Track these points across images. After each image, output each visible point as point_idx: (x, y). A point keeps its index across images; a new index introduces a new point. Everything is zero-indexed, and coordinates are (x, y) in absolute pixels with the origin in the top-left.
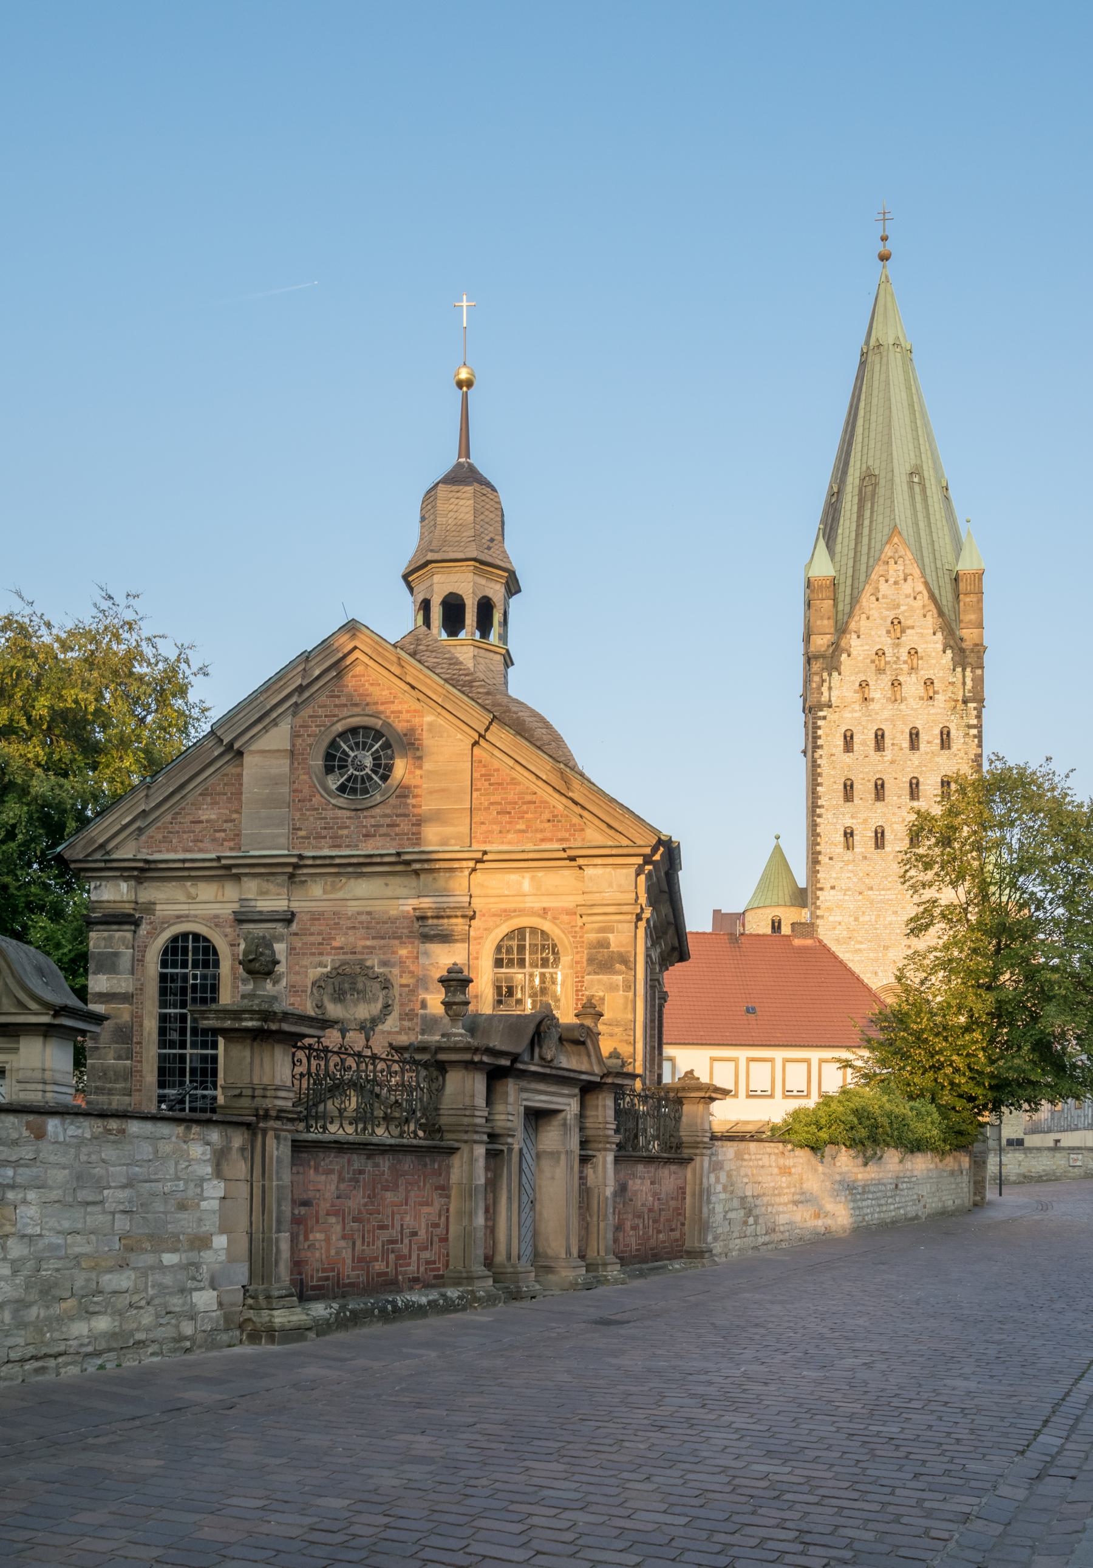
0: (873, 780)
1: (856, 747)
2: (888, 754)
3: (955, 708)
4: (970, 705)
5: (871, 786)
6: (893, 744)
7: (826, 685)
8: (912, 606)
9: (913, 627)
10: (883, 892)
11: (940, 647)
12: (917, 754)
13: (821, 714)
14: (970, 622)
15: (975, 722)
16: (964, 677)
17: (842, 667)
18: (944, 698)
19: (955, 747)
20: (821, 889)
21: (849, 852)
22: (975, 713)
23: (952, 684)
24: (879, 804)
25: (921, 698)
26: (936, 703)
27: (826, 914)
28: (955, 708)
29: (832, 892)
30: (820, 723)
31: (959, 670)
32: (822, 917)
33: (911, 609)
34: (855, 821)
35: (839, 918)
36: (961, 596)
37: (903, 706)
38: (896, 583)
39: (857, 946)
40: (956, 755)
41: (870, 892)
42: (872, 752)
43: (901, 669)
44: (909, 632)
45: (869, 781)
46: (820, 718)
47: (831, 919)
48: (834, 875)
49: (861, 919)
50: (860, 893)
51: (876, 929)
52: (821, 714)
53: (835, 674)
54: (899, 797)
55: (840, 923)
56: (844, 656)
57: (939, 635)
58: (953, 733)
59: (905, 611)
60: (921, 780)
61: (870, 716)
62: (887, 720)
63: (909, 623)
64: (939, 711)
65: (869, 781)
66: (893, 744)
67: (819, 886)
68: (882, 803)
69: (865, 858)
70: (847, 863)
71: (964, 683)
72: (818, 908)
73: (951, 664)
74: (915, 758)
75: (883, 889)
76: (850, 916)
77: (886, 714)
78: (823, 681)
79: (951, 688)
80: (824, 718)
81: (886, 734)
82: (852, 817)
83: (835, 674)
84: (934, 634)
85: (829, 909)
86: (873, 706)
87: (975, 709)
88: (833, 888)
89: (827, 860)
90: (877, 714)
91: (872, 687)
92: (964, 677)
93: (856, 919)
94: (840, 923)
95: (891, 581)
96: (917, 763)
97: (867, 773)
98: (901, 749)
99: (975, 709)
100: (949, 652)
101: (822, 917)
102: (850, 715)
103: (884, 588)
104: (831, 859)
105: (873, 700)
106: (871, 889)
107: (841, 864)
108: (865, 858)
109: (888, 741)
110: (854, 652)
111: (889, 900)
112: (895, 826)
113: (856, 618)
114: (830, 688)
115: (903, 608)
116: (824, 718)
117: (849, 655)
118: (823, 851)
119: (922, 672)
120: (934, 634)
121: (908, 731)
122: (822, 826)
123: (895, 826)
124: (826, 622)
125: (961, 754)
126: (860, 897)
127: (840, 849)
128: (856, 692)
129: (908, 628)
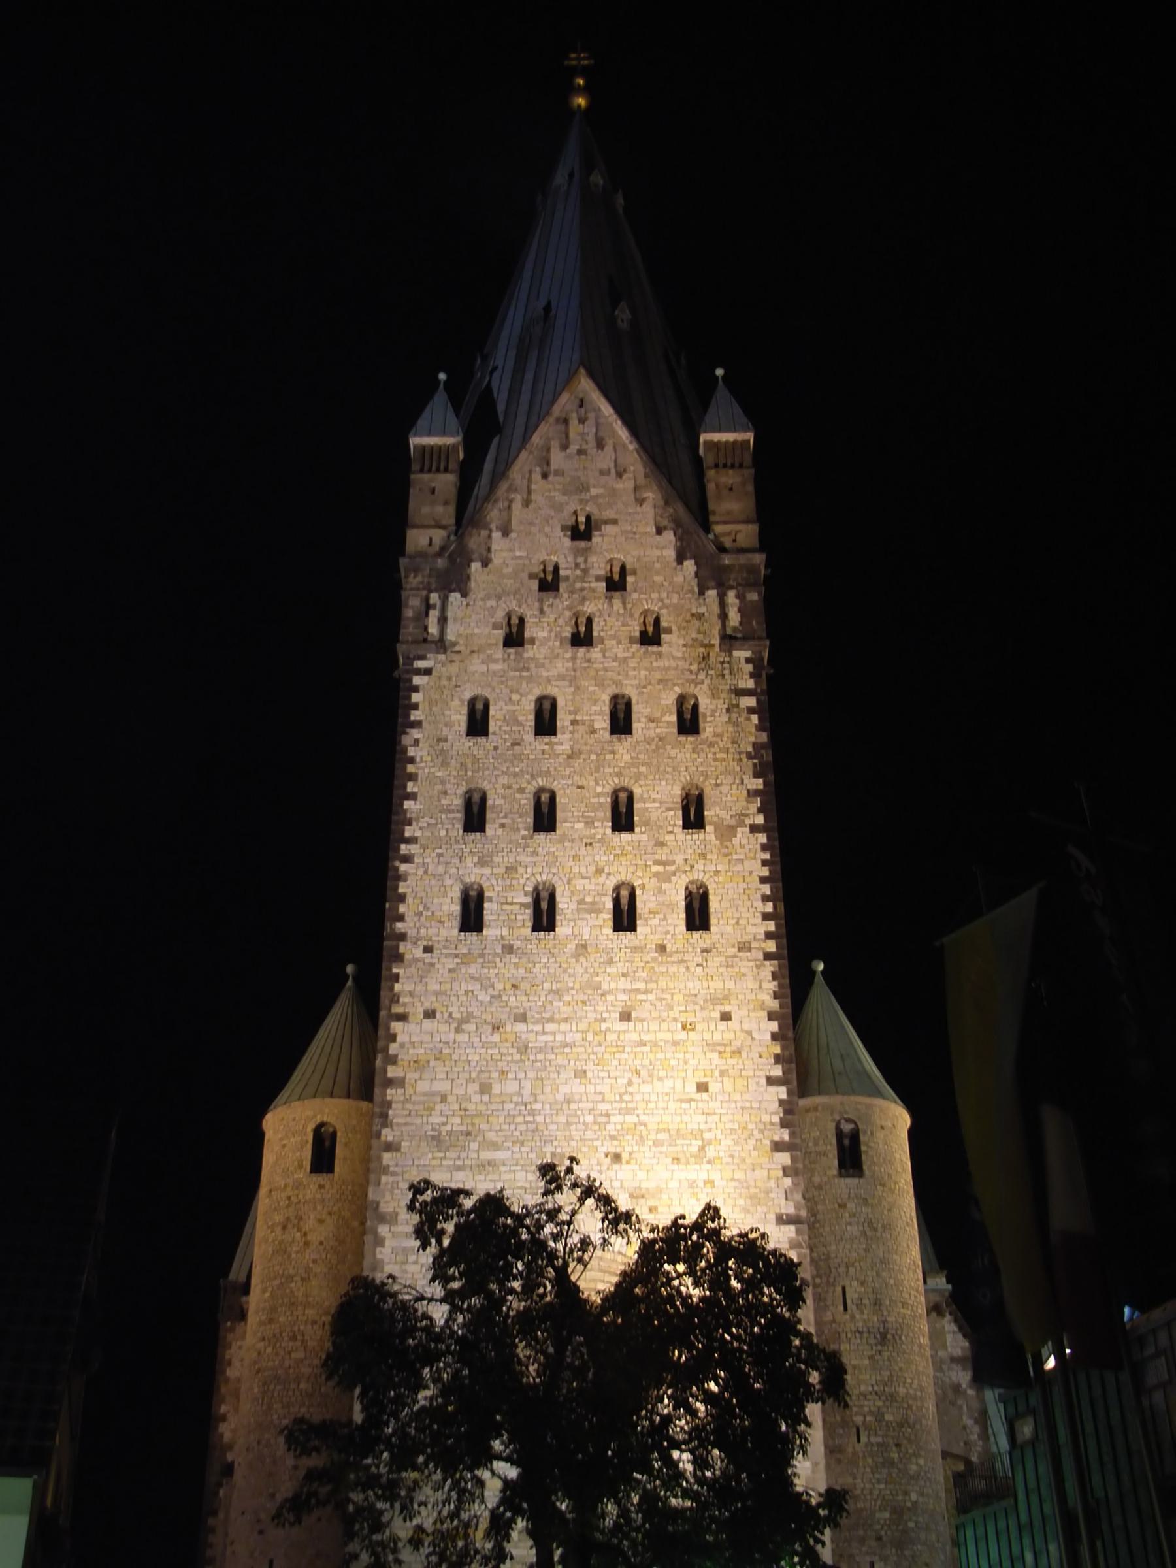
0: (531, 789)
1: (493, 726)
2: (563, 741)
3: (705, 658)
4: (736, 653)
5: (526, 802)
6: (574, 723)
7: (434, 615)
8: (614, 490)
9: (614, 522)
10: (550, 1027)
11: (671, 554)
12: (628, 741)
13: (420, 664)
14: (729, 513)
15: (750, 684)
16: (723, 605)
17: (473, 584)
18: (682, 642)
19: (708, 730)
20: (402, 1018)
21: (472, 937)
22: (750, 667)
23: (699, 617)
24: (541, 837)
25: (632, 640)
26: (664, 648)
27: (411, 1076)
28: (705, 658)
29: (428, 1024)
30: (417, 680)
31: (712, 593)
32: (400, 1083)
33: (613, 493)
34: (487, 871)
35: (442, 1086)
36: (711, 474)
37: (595, 653)
38: (580, 452)
39: (486, 1155)
40: (711, 745)
41: (520, 1027)
42: (529, 736)
43: (593, 590)
44: (608, 529)
45: (521, 790)
46: (419, 672)
47: (423, 1086)
48: (436, 987)
49: (496, 1089)
50: (496, 1028)
51: (532, 1113)
52: (420, 664)
53: (455, 597)
54: (589, 823)
55: (444, 1098)
56: (475, 566)
57: (669, 536)
58: (705, 704)
59: (598, 496)
60: (637, 791)
61: (528, 669)
62: (561, 677)
63: (609, 514)
64: (673, 664)
65: (521, 790)
66: (574, 723)
67: (397, 1009)
68: (551, 836)
69: (509, 949)
70: (466, 959)
71: (724, 616)
72: (393, 1060)
73: (694, 582)
74: (624, 748)
75: (551, 1020)
76: (470, 1080)
77: (560, 667)
78: (428, 607)
79: (697, 623)
80: (428, 672)
81: (561, 703)
82: (482, 863)
83: (455, 597)
84: (659, 531)
85: (418, 1065)
86: (529, 652)
87: (748, 661)
88: (430, 1014)
89: (418, 953)
90: (543, 665)
91: (530, 621)
92: (723, 605)
93: (485, 1089)
94: (444, 1098)
95: (574, 448)
96: (627, 757)
97: (515, 775)
98: (594, 731)
99: (748, 661)
100: (690, 566)
101: (400, 1083)
102: (484, 668)
103: (557, 459)
104: (428, 950)
105: (532, 641)
106: (522, 1018)
107: (450, 963)
108: (509, 949)
109: (563, 719)
110: (496, 560)
111: (566, 1045)
112: (580, 884)
113: (502, 504)
114: (443, 620)
115: (594, 491)
116: (428, 672)
117: (485, 563)
118: (411, 933)
119: (635, 596)
120: (659, 531)
121: (606, 698)
122: (411, 881)
123: (580, 884)
124: (440, 509)
125: (725, 742)
126: (496, 1038)
127: (452, 930)
128: (496, 626)
129: (606, 522)
